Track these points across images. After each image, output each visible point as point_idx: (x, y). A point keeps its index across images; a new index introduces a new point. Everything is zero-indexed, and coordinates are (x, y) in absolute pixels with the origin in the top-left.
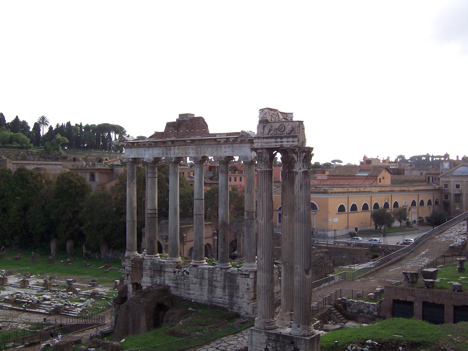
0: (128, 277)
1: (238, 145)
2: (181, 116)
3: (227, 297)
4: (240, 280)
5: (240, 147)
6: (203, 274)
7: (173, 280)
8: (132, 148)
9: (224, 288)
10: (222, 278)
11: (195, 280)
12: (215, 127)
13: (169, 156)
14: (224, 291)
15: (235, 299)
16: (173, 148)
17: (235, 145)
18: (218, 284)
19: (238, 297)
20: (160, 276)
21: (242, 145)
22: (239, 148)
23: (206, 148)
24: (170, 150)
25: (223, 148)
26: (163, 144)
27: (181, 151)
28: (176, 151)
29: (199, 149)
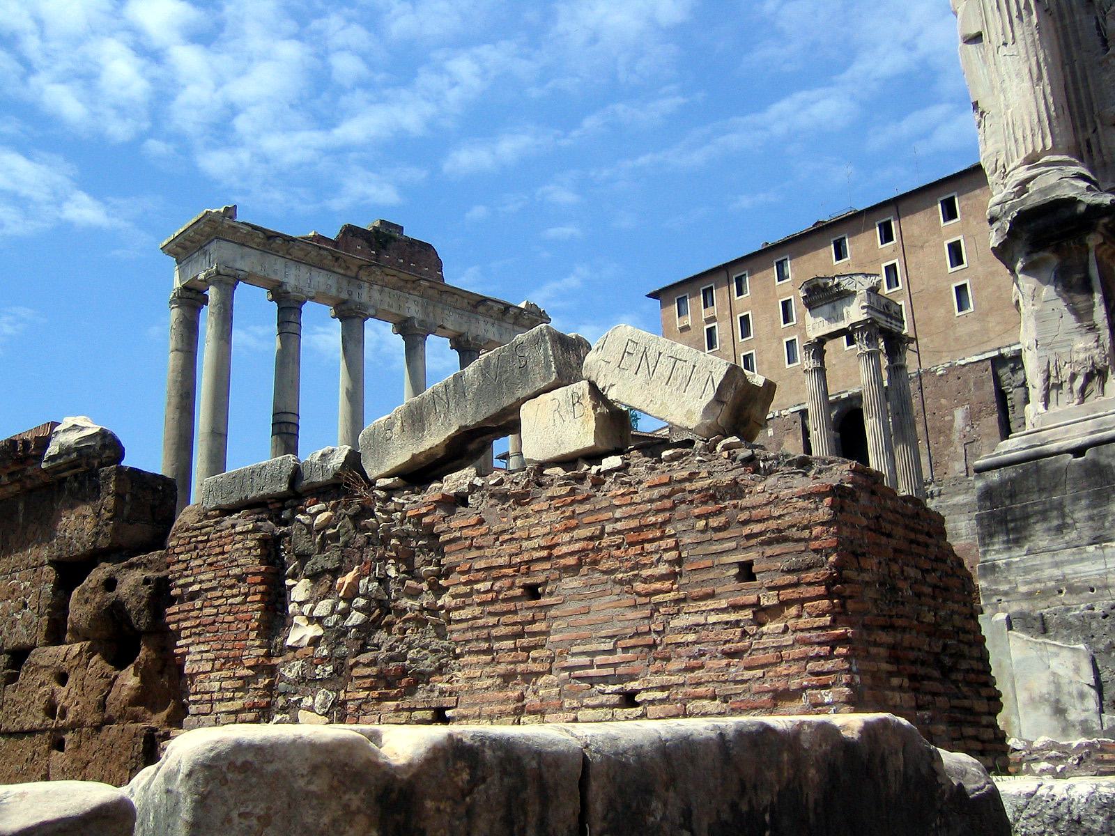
1: (510, 326)
2: (382, 222)
5: (514, 330)
8: (243, 245)
13: (355, 297)
16: (366, 285)
17: (504, 324)
21: (516, 328)
22: (512, 332)
23: (446, 312)
24: (360, 287)
25: (482, 323)
26: (345, 270)
27: (387, 299)
28: (376, 295)
29: (431, 309)
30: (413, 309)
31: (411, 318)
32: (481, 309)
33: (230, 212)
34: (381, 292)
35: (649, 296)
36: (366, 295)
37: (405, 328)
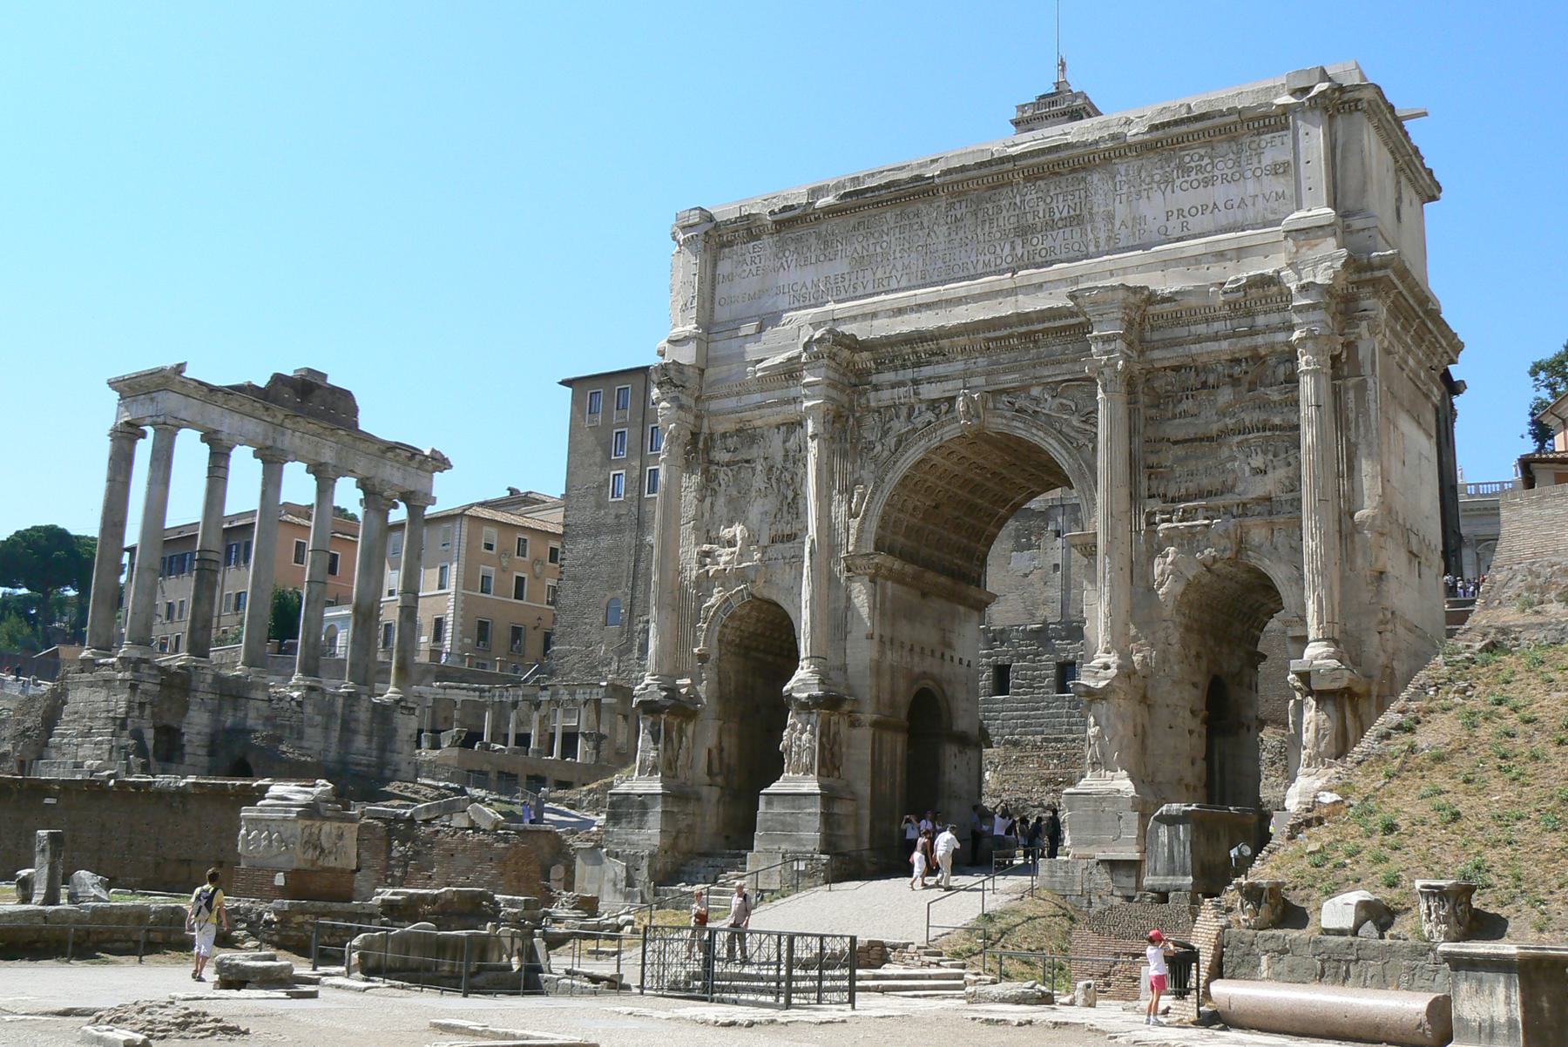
0: (142, 713)
2: (310, 371)
3: (374, 753)
4: (399, 718)
6: (332, 704)
7: (268, 719)
9: (370, 735)
10: (369, 715)
11: (318, 718)
12: (367, 422)
14: (370, 741)
15: (388, 755)
18: (362, 728)
19: (393, 751)
20: (235, 709)
28: (297, 441)
30: (328, 456)
31: (325, 464)
32: (390, 455)
33: (180, 368)
34: (301, 438)
35: (563, 383)
36: (289, 440)
37: (316, 469)
